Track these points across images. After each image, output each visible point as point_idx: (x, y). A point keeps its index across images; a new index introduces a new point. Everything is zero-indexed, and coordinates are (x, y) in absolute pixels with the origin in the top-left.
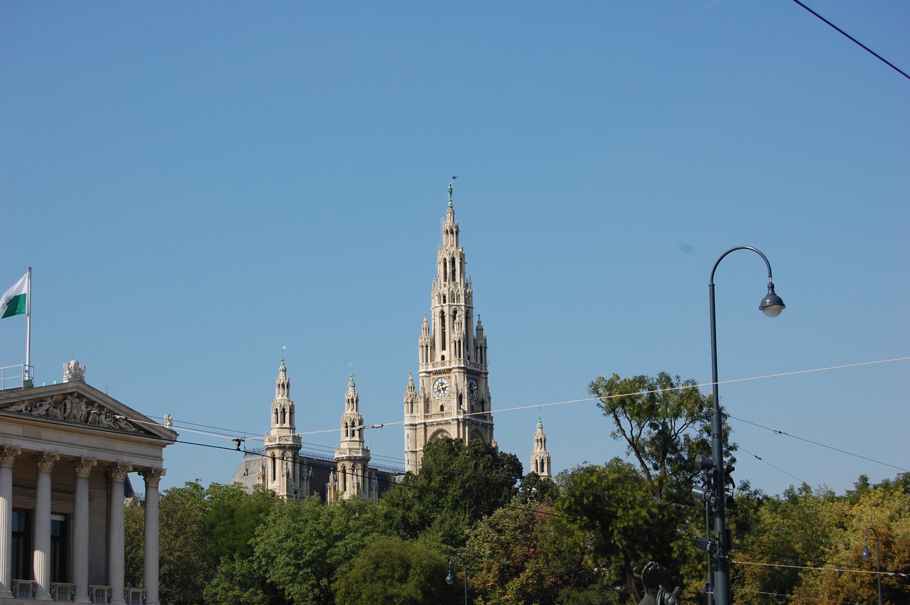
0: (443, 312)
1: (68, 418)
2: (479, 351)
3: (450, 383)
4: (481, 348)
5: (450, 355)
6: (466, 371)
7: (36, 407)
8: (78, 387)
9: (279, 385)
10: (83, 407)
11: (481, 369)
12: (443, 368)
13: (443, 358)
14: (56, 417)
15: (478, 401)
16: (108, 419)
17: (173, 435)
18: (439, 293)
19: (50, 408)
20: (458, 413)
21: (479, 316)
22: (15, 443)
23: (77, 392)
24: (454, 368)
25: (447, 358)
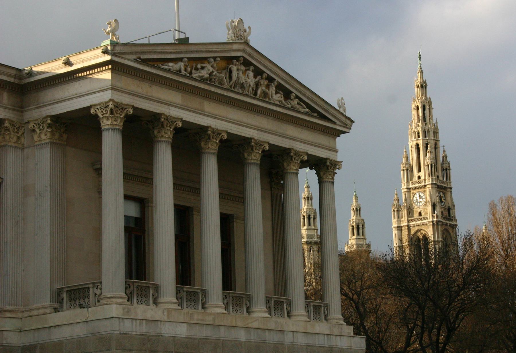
0: (417, 145)
1: (234, 88)
2: (444, 172)
3: (426, 195)
4: (446, 169)
5: (425, 175)
6: (437, 187)
7: (197, 69)
8: (244, 51)
9: (305, 198)
10: (251, 74)
11: (447, 185)
12: (420, 185)
13: (419, 177)
14: (221, 84)
15: (445, 208)
16: (278, 95)
17: (348, 122)
18: (415, 131)
19: (213, 72)
20: (433, 217)
21: (444, 147)
22: (174, 112)
23: (242, 56)
24: (428, 184)
25: (422, 178)
